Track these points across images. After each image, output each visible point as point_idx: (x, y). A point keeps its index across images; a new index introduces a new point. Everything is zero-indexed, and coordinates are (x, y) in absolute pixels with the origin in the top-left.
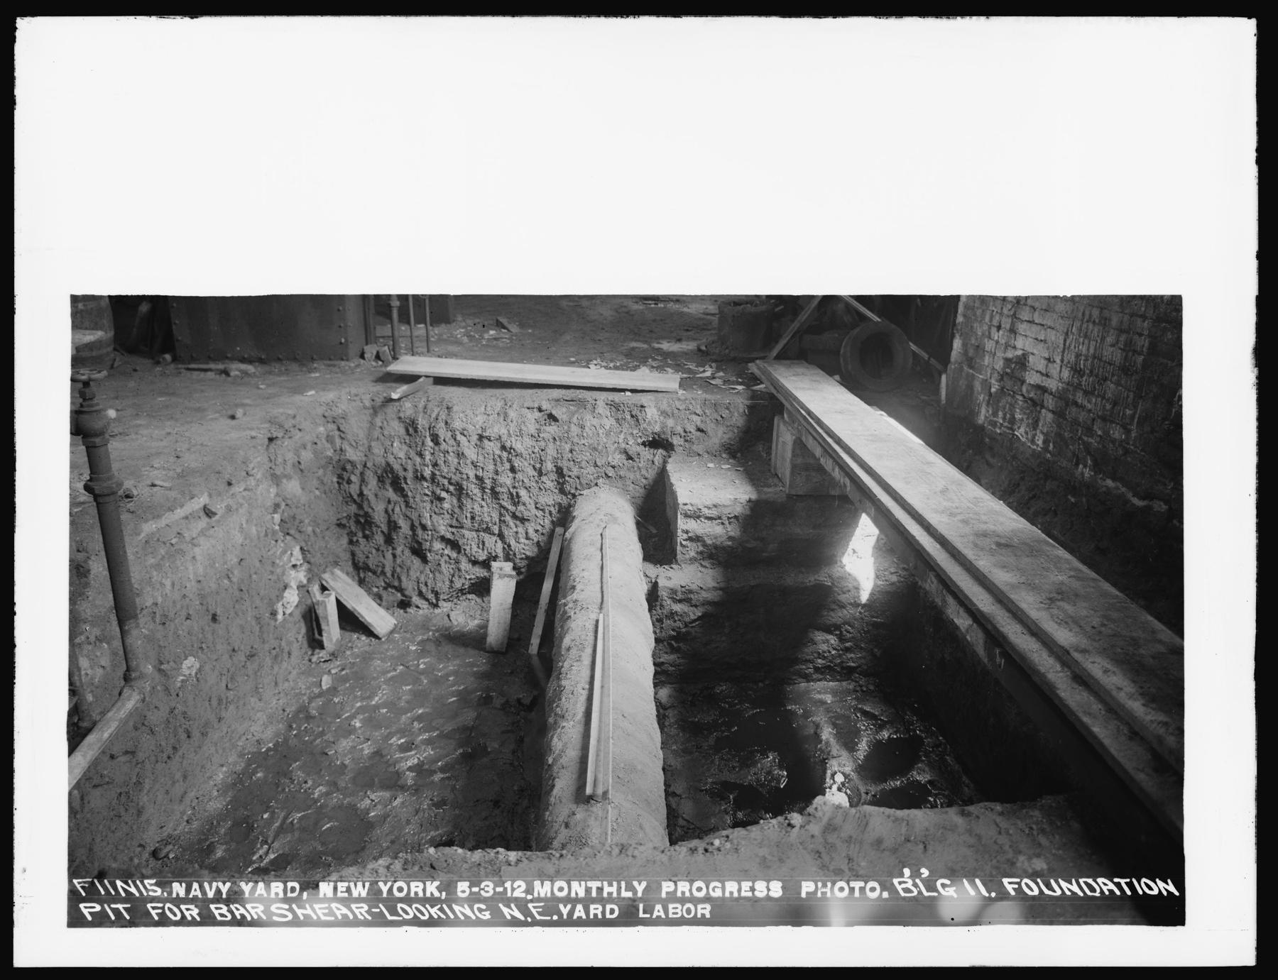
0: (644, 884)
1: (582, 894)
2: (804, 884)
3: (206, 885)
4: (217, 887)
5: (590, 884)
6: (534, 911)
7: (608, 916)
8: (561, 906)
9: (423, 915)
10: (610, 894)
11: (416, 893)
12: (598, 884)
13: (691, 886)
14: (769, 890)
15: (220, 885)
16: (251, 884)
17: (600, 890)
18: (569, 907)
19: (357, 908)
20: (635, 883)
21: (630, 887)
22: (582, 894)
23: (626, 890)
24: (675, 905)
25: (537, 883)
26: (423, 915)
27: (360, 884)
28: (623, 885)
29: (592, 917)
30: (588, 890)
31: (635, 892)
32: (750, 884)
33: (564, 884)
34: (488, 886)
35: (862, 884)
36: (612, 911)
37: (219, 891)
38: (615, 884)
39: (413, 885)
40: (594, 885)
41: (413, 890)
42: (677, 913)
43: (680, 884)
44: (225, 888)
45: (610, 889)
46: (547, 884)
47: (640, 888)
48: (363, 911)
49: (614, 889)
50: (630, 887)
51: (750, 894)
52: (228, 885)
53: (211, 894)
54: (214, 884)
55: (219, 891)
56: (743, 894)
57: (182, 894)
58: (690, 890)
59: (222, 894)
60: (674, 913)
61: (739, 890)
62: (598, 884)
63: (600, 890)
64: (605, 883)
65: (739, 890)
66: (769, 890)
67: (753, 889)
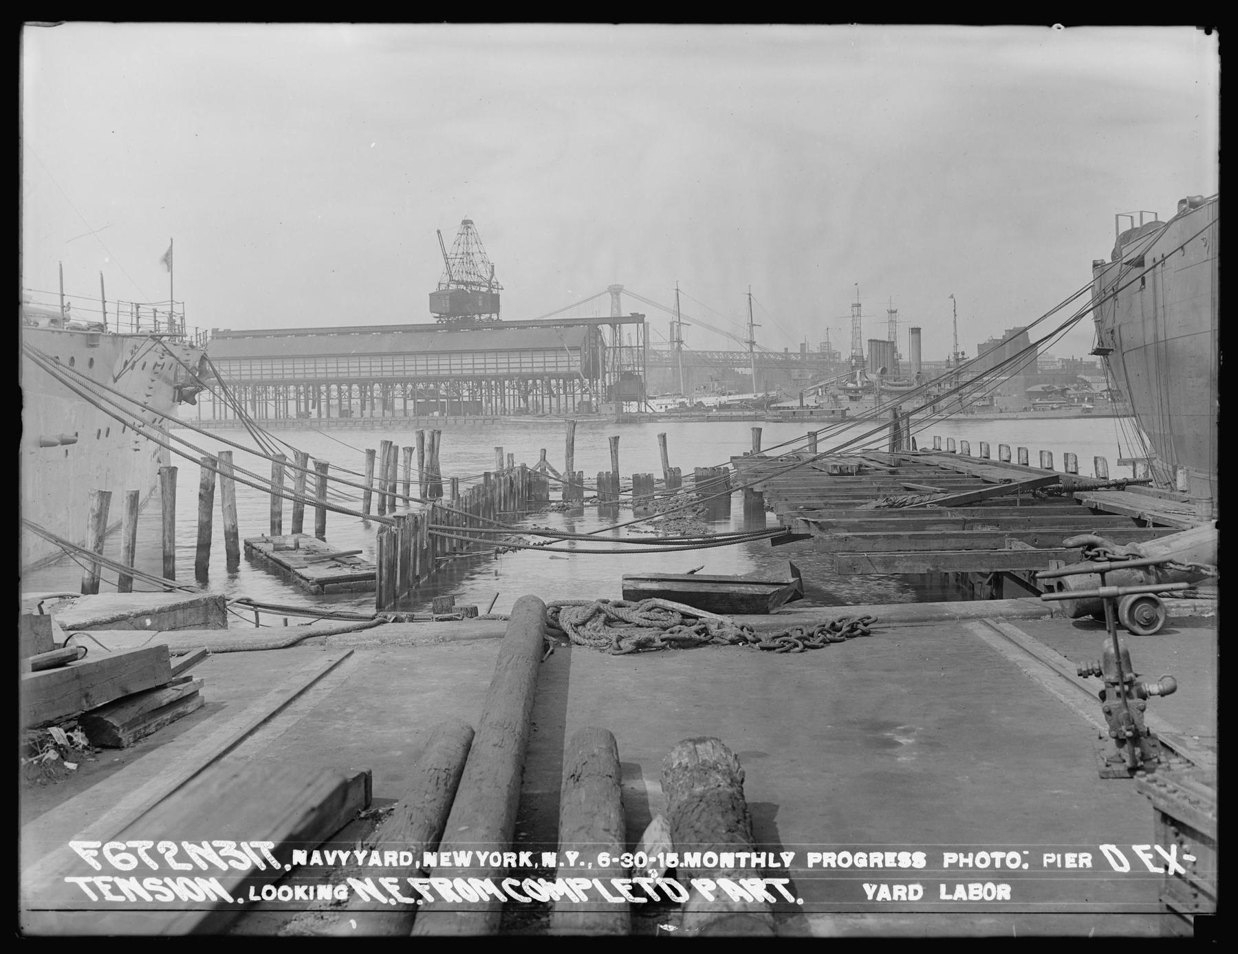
2: (947, 855)
5: (739, 855)
12: (747, 855)
13: (837, 854)
14: (911, 858)
17: (748, 860)
20: (783, 855)
21: (778, 859)
22: (731, 865)
23: (774, 862)
25: (687, 855)
28: (771, 856)
35: (1002, 855)
40: (743, 856)
43: (826, 855)
51: (895, 865)
56: (887, 865)
58: (836, 861)
61: (884, 861)
63: (748, 860)
67: (897, 861)
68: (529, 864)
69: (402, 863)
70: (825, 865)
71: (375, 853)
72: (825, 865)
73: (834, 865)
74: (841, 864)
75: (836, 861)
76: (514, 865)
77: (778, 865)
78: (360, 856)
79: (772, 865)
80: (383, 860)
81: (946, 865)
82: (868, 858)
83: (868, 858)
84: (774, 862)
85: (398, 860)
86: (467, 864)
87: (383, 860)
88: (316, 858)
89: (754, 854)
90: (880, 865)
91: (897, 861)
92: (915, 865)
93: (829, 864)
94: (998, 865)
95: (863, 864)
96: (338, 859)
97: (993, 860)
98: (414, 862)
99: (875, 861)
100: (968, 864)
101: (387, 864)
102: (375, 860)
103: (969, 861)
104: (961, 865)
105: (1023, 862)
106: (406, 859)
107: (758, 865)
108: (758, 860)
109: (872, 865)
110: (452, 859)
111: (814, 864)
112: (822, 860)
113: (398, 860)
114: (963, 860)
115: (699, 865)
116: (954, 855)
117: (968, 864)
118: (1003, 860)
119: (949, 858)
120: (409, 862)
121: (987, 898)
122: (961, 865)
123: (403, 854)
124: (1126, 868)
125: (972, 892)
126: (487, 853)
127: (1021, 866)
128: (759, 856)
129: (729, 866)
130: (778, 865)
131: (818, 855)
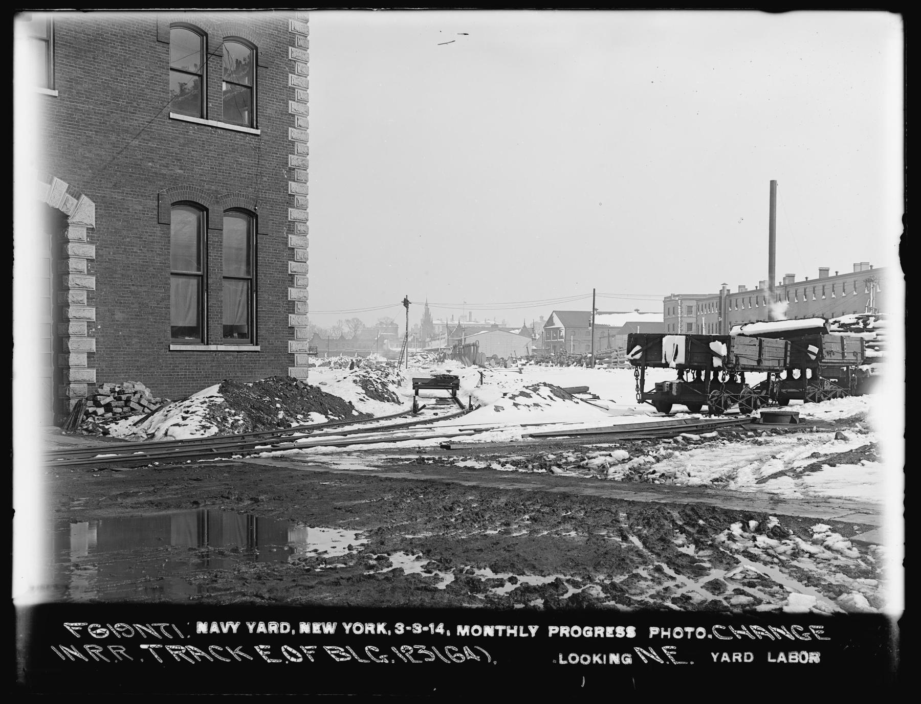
0: (537, 627)
1: (491, 634)
3: (222, 624)
5: (498, 627)
7: (746, 660)
14: (625, 631)
16: (254, 624)
17: (504, 631)
20: (530, 627)
21: (526, 631)
22: (491, 634)
23: (523, 633)
25: (459, 628)
28: (522, 628)
29: (734, 661)
30: (496, 631)
31: (530, 633)
32: (613, 628)
37: (230, 629)
38: (516, 627)
40: (500, 628)
43: (562, 628)
44: (235, 627)
45: (512, 631)
46: (467, 628)
47: (533, 630)
49: (514, 632)
50: (526, 631)
51: (613, 636)
53: (225, 630)
54: (227, 625)
55: (230, 629)
58: (570, 633)
61: (605, 633)
63: (504, 631)
65: (605, 633)
67: (614, 632)
68: (384, 632)
69: (282, 631)
70: (561, 635)
72: (561, 635)
73: (568, 635)
74: (573, 635)
75: (570, 633)
76: (373, 632)
77: (526, 635)
79: (522, 635)
82: (593, 631)
83: (593, 631)
84: (523, 633)
85: (279, 628)
86: (332, 631)
88: (214, 628)
89: (508, 627)
90: (602, 636)
91: (614, 632)
92: (628, 636)
93: (564, 634)
94: (689, 637)
95: (590, 634)
96: (230, 628)
98: (291, 631)
99: (599, 632)
102: (261, 628)
103: (668, 633)
104: (662, 637)
105: (707, 633)
106: (285, 628)
108: (512, 631)
109: (596, 636)
110: (321, 628)
111: (653, 635)
112: (559, 632)
113: (279, 628)
114: (663, 633)
115: (468, 634)
116: (657, 629)
118: (693, 634)
119: (654, 631)
120: (288, 630)
121: (801, 661)
122: (662, 637)
123: (283, 624)
124: (794, 639)
125: (791, 657)
126: (350, 624)
128: (512, 628)
129: (490, 635)
130: (526, 635)
131: (557, 628)
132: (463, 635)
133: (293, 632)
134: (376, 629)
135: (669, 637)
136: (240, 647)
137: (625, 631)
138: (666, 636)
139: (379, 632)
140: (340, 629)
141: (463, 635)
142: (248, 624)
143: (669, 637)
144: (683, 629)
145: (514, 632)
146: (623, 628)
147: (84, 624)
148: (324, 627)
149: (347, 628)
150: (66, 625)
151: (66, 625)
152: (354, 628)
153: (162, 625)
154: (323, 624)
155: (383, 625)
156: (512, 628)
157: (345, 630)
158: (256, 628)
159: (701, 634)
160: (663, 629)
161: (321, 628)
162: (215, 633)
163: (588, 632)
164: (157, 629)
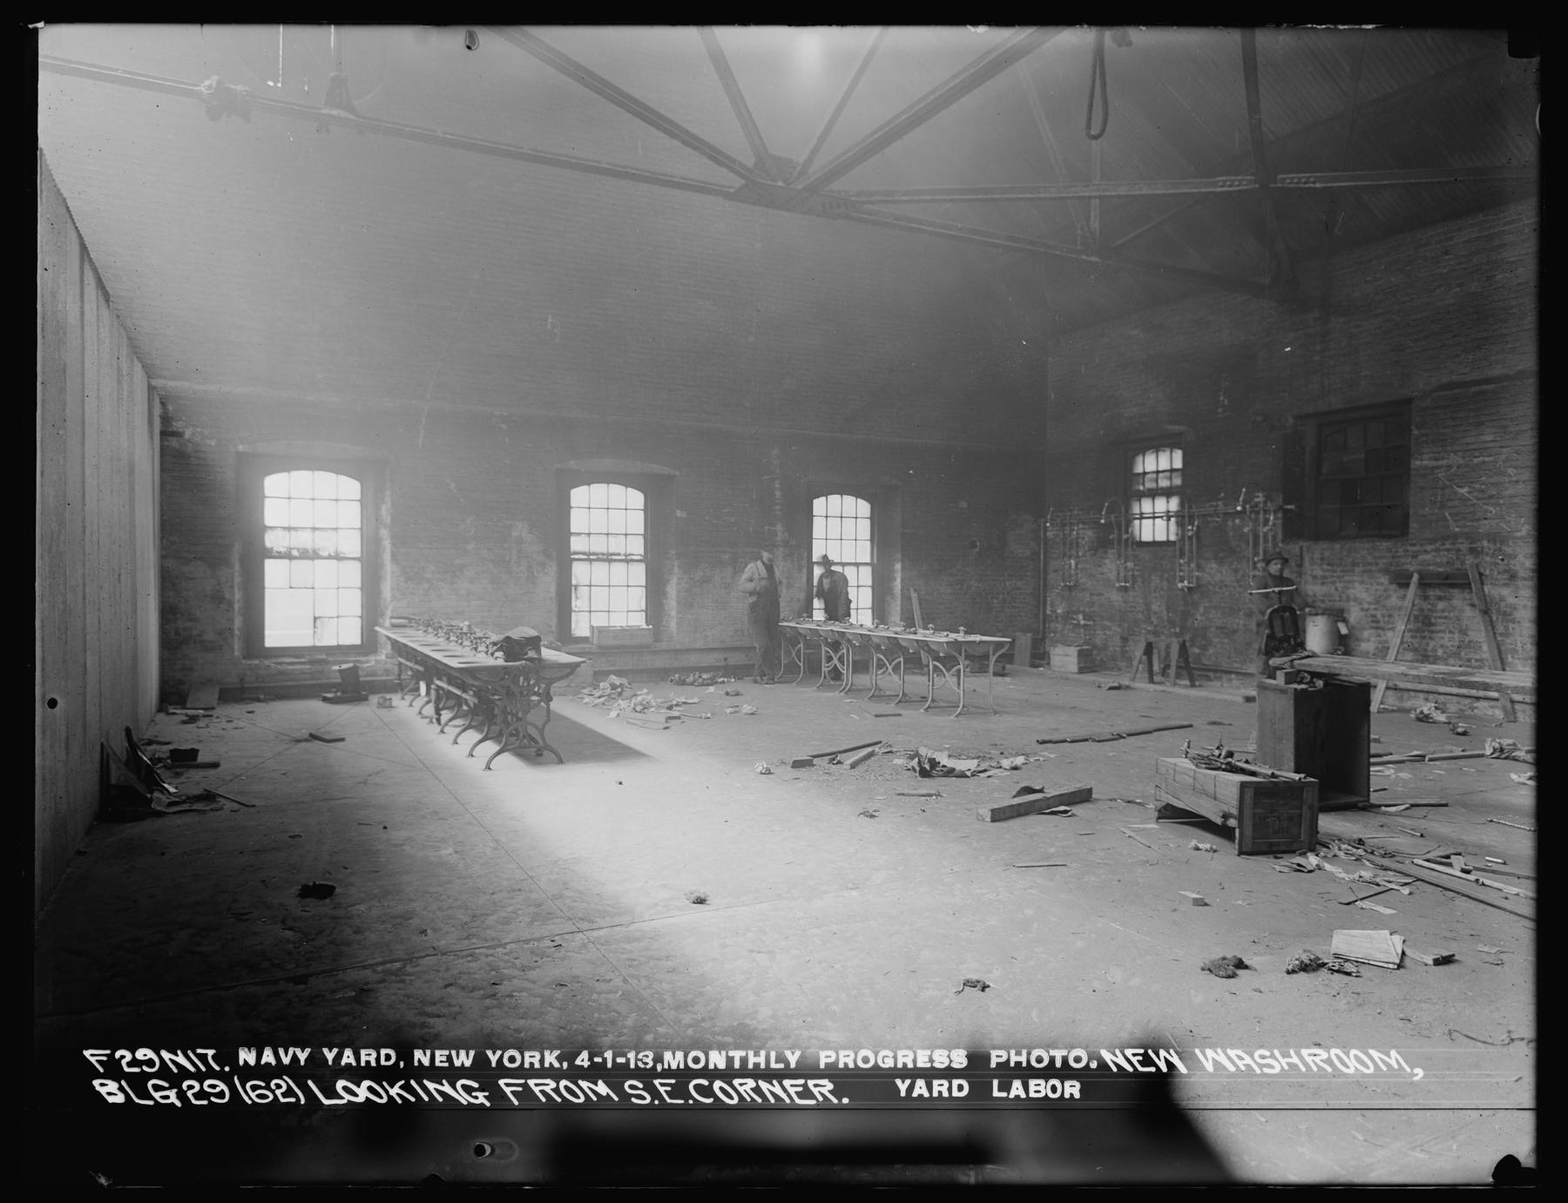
1: (722, 1065)
3: (281, 1051)
4: (294, 1053)
6: (662, 1090)
8: (898, 1082)
9: (731, 1097)
10: (757, 1065)
11: (532, 1064)
12: (743, 1053)
14: (949, 1056)
15: (298, 1051)
17: (744, 1061)
18: (908, 1082)
19: (536, 1085)
23: (776, 1062)
24: (1038, 1081)
26: (731, 1097)
27: (463, 1053)
30: (730, 1060)
32: (929, 1052)
33: (702, 1056)
34: (647, 1056)
36: (960, 1088)
37: (295, 1058)
39: (527, 1054)
40: (737, 1055)
41: (527, 1061)
42: (1039, 1092)
43: (842, 1053)
44: (303, 1056)
45: (757, 1060)
46: (680, 1055)
48: (547, 1089)
51: (929, 1065)
52: (308, 1050)
53: (286, 1060)
54: (291, 1051)
55: (295, 1058)
56: (920, 1065)
57: (252, 1061)
59: (299, 1061)
60: (1036, 1092)
61: (915, 1061)
62: (743, 1053)
63: (744, 1061)
64: (751, 1053)
66: (951, 1061)
67: (931, 1061)
69: (383, 1062)
71: (348, 1052)
78: (330, 1055)
79: (773, 1065)
80: (358, 1059)
81: (993, 1065)
82: (895, 1058)
83: (895, 1058)
84: (776, 1062)
86: (468, 1063)
87: (358, 1059)
97: (1052, 1060)
98: (397, 1063)
100: (1021, 1063)
101: (363, 1064)
102: (348, 1057)
103: (1023, 1059)
104: (1012, 1064)
106: (388, 1057)
107: (757, 1065)
113: (378, 1059)
114: (1014, 1059)
115: (682, 1066)
117: (1021, 1063)
118: (1065, 1060)
122: (1012, 1064)
123: (383, 1052)
126: (499, 1053)
127: (1088, 1064)
130: (781, 1066)
132: (674, 1066)
133: (402, 1064)
134: (542, 1061)
135: (1024, 1065)
136: (487, 1094)
137: (949, 1056)
138: (1018, 1064)
139: (547, 1065)
140: (481, 1060)
141: (674, 1066)
142: (325, 1050)
143: (1024, 1065)
144: (1048, 1052)
145: (761, 1060)
146: (946, 1053)
147: (108, 1052)
148: (454, 1053)
149: (493, 1058)
150: (87, 1053)
151: (87, 1053)
152: (506, 1056)
153: (211, 1052)
154: (454, 1053)
155: (557, 1053)
156: (757, 1054)
157: (490, 1062)
158: (339, 1056)
159: (1078, 1060)
160: (1013, 1052)
161: (449, 1059)
162: (268, 1064)
163: (886, 1060)
164: (203, 1058)
